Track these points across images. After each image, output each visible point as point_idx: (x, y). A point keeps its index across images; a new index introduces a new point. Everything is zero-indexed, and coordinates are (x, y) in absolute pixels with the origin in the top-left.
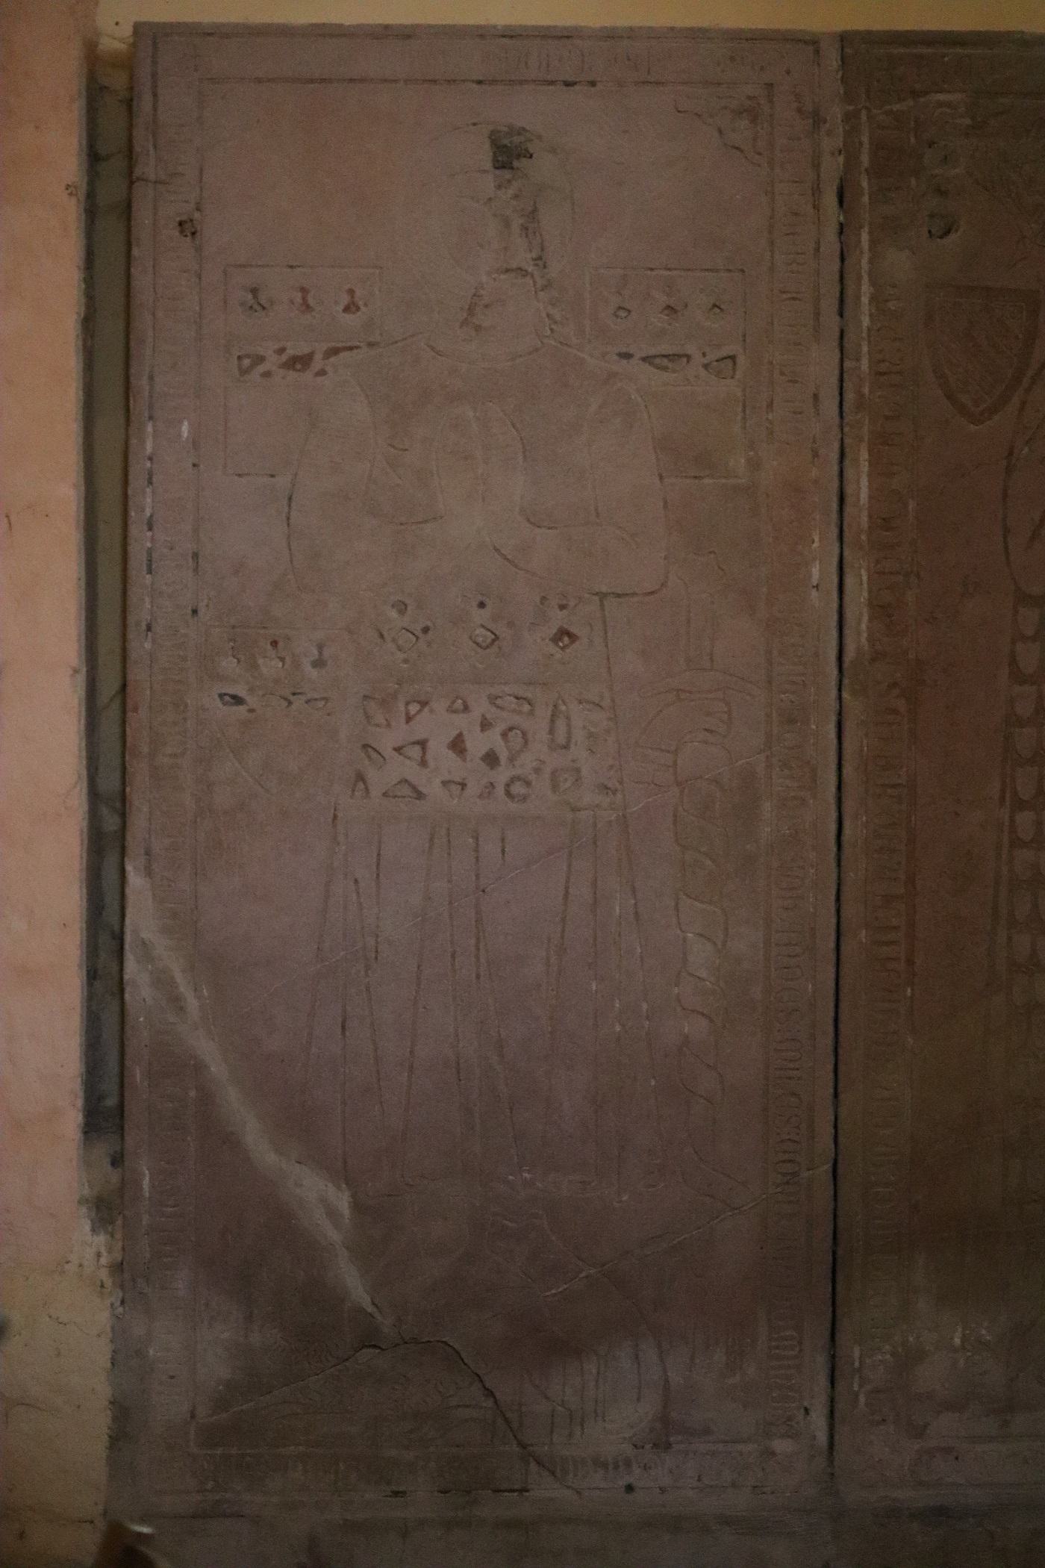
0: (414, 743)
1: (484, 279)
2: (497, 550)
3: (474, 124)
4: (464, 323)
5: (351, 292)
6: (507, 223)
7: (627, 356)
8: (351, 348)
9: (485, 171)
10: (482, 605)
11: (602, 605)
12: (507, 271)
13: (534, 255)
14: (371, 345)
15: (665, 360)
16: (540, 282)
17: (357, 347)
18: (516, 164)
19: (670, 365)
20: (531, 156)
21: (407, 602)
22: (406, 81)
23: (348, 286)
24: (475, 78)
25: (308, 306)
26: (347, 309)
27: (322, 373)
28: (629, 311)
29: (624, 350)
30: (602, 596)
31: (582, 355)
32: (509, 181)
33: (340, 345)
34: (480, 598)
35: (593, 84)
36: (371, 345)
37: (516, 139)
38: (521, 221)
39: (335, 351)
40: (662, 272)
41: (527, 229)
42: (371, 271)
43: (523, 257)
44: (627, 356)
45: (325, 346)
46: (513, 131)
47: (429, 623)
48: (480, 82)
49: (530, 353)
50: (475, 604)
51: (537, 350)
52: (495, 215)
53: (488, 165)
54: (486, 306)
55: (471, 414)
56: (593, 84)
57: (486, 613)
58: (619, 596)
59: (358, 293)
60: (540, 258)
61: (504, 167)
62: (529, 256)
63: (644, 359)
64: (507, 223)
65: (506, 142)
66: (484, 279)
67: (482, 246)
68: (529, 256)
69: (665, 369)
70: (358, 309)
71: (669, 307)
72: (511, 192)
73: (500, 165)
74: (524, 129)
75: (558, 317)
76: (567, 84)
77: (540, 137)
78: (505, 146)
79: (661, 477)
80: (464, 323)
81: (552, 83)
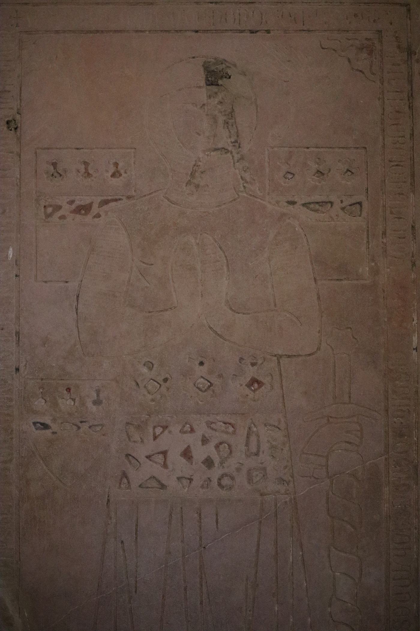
0: (159, 453)
1: (201, 155)
2: (211, 328)
3: (194, 57)
4: (189, 183)
5: (116, 164)
6: (215, 119)
7: (293, 203)
8: (116, 200)
9: (200, 87)
10: (201, 364)
11: (279, 362)
12: (216, 150)
13: (233, 140)
14: (129, 198)
15: (317, 206)
16: (237, 157)
17: (120, 199)
18: (220, 82)
19: (320, 208)
20: (230, 78)
21: (154, 363)
22: (150, 31)
23: (114, 161)
24: (194, 29)
25: (89, 174)
26: (113, 175)
27: (98, 216)
28: (294, 175)
29: (290, 199)
30: (279, 357)
31: (264, 203)
32: (216, 93)
33: (110, 198)
34: (200, 359)
35: (268, 32)
36: (129, 198)
37: (220, 67)
38: (225, 118)
39: (106, 202)
40: (314, 149)
41: (227, 123)
42: (129, 150)
43: (225, 141)
44: (293, 203)
45: (99, 199)
46: (218, 61)
47: (168, 376)
48: (197, 32)
49: (231, 202)
50: (197, 363)
51: (235, 200)
52: (207, 115)
53: (203, 83)
54: (202, 173)
55: (193, 241)
56: (268, 32)
58: (289, 356)
59: (121, 164)
60: (236, 141)
61: (212, 84)
62: (229, 140)
63: (304, 205)
64: (215, 119)
65: (213, 68)
66: (201, 155)
67: (199, 134)
68: (229, 140)
69: (316, 211)
70: (121, 175)
71: (318, 171)
72: (216, 101)
73: (210, 83)
74: (225, 60)
75: (248, 180)
76: (252, 32)
77: (235, 66)
78: (213, 71)
79: (315, 280)
80: (189, 183)
81: (242, 31)
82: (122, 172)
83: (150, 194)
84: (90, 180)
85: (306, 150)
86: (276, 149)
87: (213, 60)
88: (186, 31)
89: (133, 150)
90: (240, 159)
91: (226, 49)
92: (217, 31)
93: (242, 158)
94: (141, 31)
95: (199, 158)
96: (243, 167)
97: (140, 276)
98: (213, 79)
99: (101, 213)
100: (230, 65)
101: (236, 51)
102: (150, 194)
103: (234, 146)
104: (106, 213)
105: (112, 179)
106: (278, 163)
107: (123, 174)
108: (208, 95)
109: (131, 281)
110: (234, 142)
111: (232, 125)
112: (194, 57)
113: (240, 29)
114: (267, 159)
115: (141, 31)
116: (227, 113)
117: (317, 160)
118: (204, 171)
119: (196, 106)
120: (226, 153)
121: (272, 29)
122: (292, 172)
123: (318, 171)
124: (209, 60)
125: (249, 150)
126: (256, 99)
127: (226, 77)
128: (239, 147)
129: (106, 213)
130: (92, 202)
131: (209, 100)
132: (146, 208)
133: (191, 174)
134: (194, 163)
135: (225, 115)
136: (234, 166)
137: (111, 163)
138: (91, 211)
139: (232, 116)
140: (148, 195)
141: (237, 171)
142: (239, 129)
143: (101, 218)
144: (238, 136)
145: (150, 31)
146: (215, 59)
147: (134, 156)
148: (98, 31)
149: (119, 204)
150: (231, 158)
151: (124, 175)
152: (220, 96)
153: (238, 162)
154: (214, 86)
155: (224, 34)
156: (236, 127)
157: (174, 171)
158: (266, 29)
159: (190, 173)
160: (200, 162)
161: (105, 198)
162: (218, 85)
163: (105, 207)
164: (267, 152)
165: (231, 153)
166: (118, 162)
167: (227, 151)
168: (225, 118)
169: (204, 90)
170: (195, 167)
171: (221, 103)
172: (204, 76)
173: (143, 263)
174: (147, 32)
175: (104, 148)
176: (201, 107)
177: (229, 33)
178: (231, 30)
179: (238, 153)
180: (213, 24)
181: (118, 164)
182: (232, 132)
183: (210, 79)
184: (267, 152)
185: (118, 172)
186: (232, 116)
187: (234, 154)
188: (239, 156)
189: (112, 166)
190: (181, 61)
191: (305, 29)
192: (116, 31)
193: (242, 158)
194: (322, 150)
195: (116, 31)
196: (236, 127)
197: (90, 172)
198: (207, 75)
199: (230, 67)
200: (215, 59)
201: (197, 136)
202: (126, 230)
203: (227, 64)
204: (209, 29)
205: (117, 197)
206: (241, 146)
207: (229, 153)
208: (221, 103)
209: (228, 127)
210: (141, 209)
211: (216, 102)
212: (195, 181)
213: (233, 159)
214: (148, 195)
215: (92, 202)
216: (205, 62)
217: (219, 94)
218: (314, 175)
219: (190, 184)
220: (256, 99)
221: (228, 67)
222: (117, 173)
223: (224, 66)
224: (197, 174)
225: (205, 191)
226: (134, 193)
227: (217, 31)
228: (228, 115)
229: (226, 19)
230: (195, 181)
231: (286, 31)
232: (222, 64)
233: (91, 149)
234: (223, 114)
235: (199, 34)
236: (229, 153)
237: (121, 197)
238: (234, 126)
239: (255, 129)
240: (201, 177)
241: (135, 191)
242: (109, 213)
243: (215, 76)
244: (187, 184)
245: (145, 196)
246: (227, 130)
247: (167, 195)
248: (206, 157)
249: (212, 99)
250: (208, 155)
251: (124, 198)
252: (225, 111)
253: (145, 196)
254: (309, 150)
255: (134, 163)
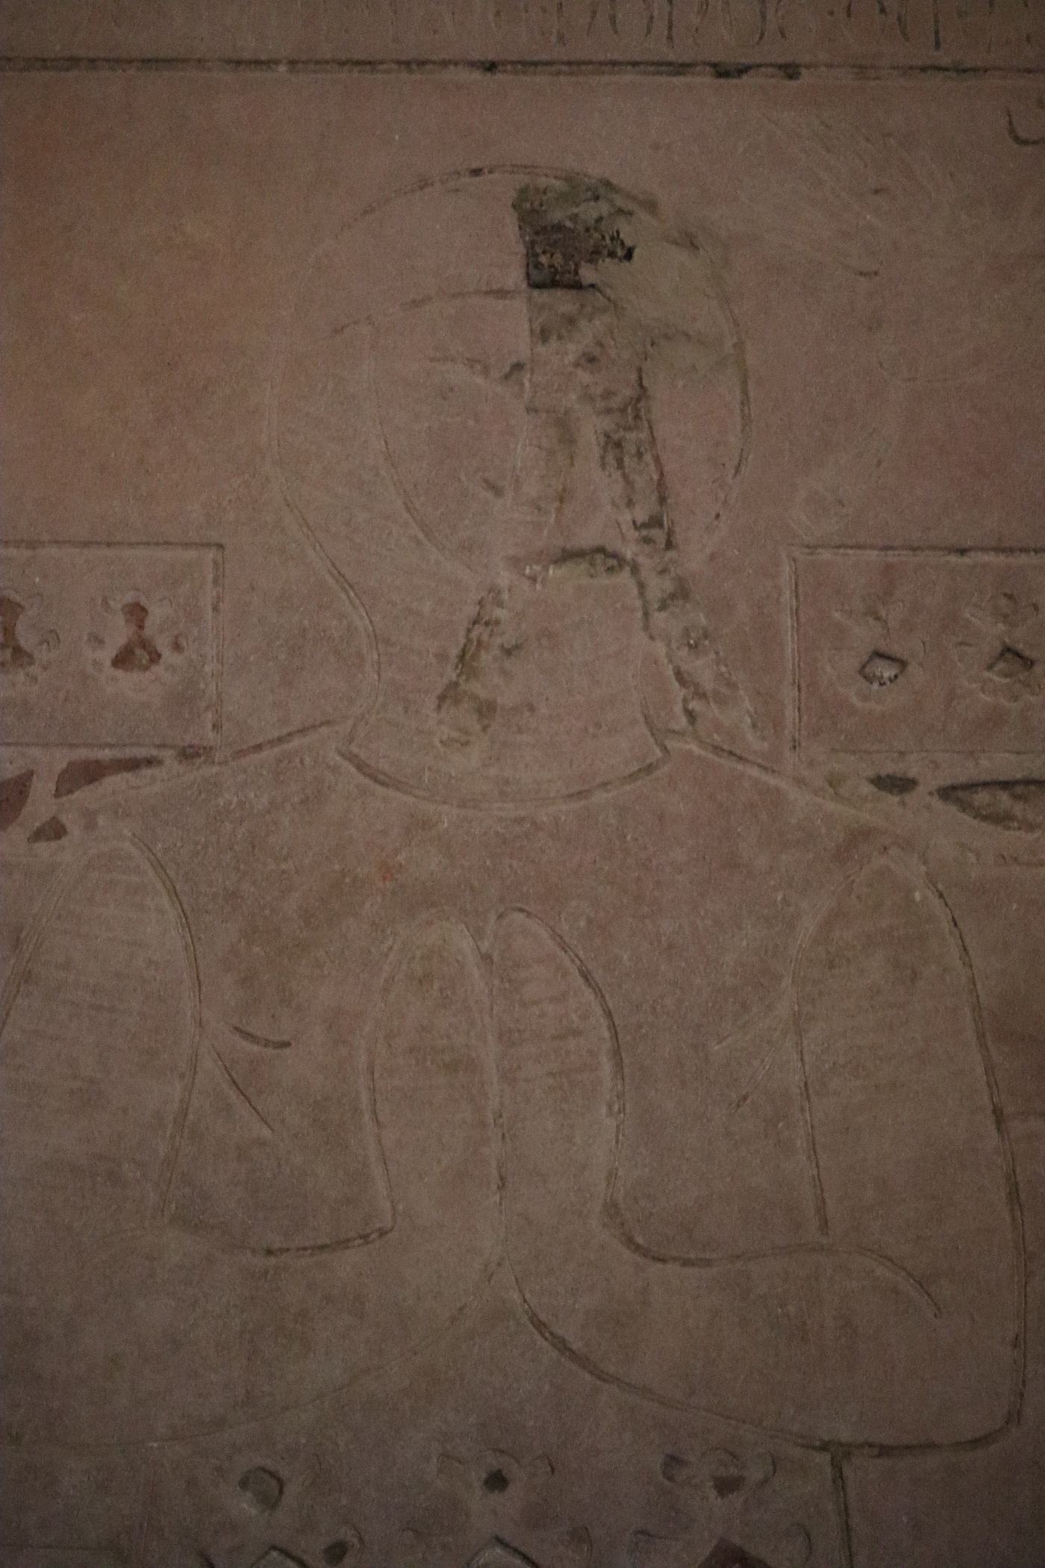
1: (504, 577)
2: (540, 1325)
3: (476, 172)
4: (449, 695)
5: (137, 613)
6: (565, 430)
7: (899, 784)
8: (133, 765)
9: (502, 293)
10: (497, 1481)
11: (839, 1477)
12: (568, 556)
13: (642, 516)
14: (188, 754)
15: (1004, 798)
16: (658, 587)
17: (150, 762)
18: (587, 274)
19: (1018, 809)
20: (629, 255)
21: (284, 1473)
22: (292, 63)
23: (129, 597)
24: (476, 56)
25: (18, 651)
26: (123, 660)
27: (54, 830)
28: (903, 664)
29: (889, 768)
30: (840, 1453)
31: (773, 781)
32: (571, 321)
33: (106, 754)
34: (493, 1462)
35: (790, 70)
36: (188, 754)
37: (589, 211)
38: (606, 423)
39: (90, 773)
40: (990, 558)
41: (618, 445)
42: (191, 554)
43: (608, 518)
44: (899, 784)
45: (61, 759)
46: (577, 188)
47: (346, 1534)
48: (491, 67)
49: (632, 777)
50: (477, 1476)
51: (649, 769)
52: (531, 410)
53: (514, 276)
54: (508, 652)
55: (466, 944)
56: (790, 70)
57: (512, 1501)
58: (884, 1451)
59: (157, 613)
60: (655, 522)
61: (554, 284)
62: (626, 517)
63: (947, 793)
64: (565, 430)
65: (557, 215)
66: (504, 577)
67: (498, 492)
68: (626, 517)
69: (1001, 819)
70: (155, 657)
71: (1009, 652)
72: (573, 350)
73: (545, 279)
74: (608, 184)
75: (708, 684)
76: (722, 72)
77: (651, 206)
78: (559, 228)
79: (998, 1114)
80: (449, 695)
81: (681, 68)
82: (163, 644)
83: (280, 740)
84: (21, 677)
85: (953, 559)
86: (826, 555)
87: (558, 184)
88: (445, 63)
89: (211, 554)
90: (673, 596)
91: (613, 138)
92: (575, 66)
93: (681, 593)
94: (257, 63)
95: (494, 590)
96: (686, 632)
97: (232, 1095)
98: (558, 260)
99: (65, 819)
100: (630, 206)
101: (656, 147)
102: (280, 740)
103: (647, 540)
104: (90, 820)
105: (120, 673)
106: (837, 615)
107: (167, 654)
108: (537, 326)
109: (191, 1117)
110: (646, 525)
111: (640, 455)
112: (476, 172)
113: (672, 57)
114: (787, 595)
115: (257, 63)
116: (616, 402)
117: (1003, 601)
118: (517, 647)
119: (486, 371)
120: (610, 570)
121: (807, 58)
122: (896, 649)
123: (1009, 652)
124: (542, 182)
125: (713, 557)
126: (739, 346)
127: (612, 254)
128: (669, 545)
129: (90, 820)
130: (30, 774)
131: (541, 349)
132: (265, 800)
133: (462, 657)
134: (472, 610)
135: (608, 411)
136: (646, 627)
137: (116, 605)
138: (26, 810)
139: (637, 417)
140: (272, 743)
141: (660, 648)
142: (668, 468)
143: (65, 841)
144: (662, 500)
145: (292, 63)
146: (568, 179)
147: (215, 581)
148: (74, 62)
149: (147, 785)
150: (635, 591)
151: (168, 655)
152: (589, 331)
153: (663, 607)
154: (559, 293)
155: (605, 79)
156: (657, 459)
157: (387, 642)
158: (781, 60)
159: (454, 652)
160: (500, 604)
161: (83, 754)
162: (577, 286)
163: (85, 796)
164: (786, 569)
165: (635, 569)
166: (143, 601)
167: (614, 561)
168: (606, 423)
169: (519, 306)
170: (478, 630)
171: (592, 360)
172: (521, 249)
173: (248, 1036)
174: (282, 68)
175: (86, 544)
176: (507, 377)
177: (628, 77)
178: (635, 64)
179: (664, 571)
180: (561, 38)
181: (143, 610)
182: (639, 481)
183: (544, 259)
184: (786, 569)
185: (144, 644)
186: (637, 417)
187: (644, 573)
188: (668, 585)
189: (120, 620)
190: (424, 184)
191: (946, 61)
192: (148, 63)
193: (681, 593)
194: (1023, 559)
195: (148, 63)
196: (657, 459)
197: (22, 643)
198: (533, 243)
199: (631, 213)
200: (568, 179)
201: (490, 495)
202: (174, 893)
203: (620, 202)
204: (545, 57)
205: (141, 752)
206: (678, 538)
207: (626, 573)
208: (592, 360)
209: (620, 463)
210: (241, 804)
211: (571, 358)
212: (476, 687)
213: (642, 594)
214: (272, 743)
215: (30, 774)
216: (523, 192)
217: (583, 323)
218: (990, 667)
219: (456, 702)
220: (739, 346)
221: (621, 211)
222: (138, 652)
223: (604, 208)
224: (485, 658)
225: (520, 731)
226: (211, 735)
227: (575, 66)
228: (623, 410)
229: (613, 19)
230: (476, 687)
231: (861, 70)
232: (597, 198)
233: (32, 545)
234: (600, 404)
235: (499, 76)
236: (626, 573)
237: (154, 752)
238: (648, 457)
239: (737, 470)
240: (503, 672)
241: (216, 727)
242: (101, 821)
243: (565, 250)
244: (442, 698)
245: (258, 748)
246: (617, 475)
247: (355, 749)
248: (526, 585)
249: (554, 343)
250: (533, 579)
251: (168, 755)
252: (608, 394)
253: (258, 748)
254: (966, 560)
255: (215, 609)
